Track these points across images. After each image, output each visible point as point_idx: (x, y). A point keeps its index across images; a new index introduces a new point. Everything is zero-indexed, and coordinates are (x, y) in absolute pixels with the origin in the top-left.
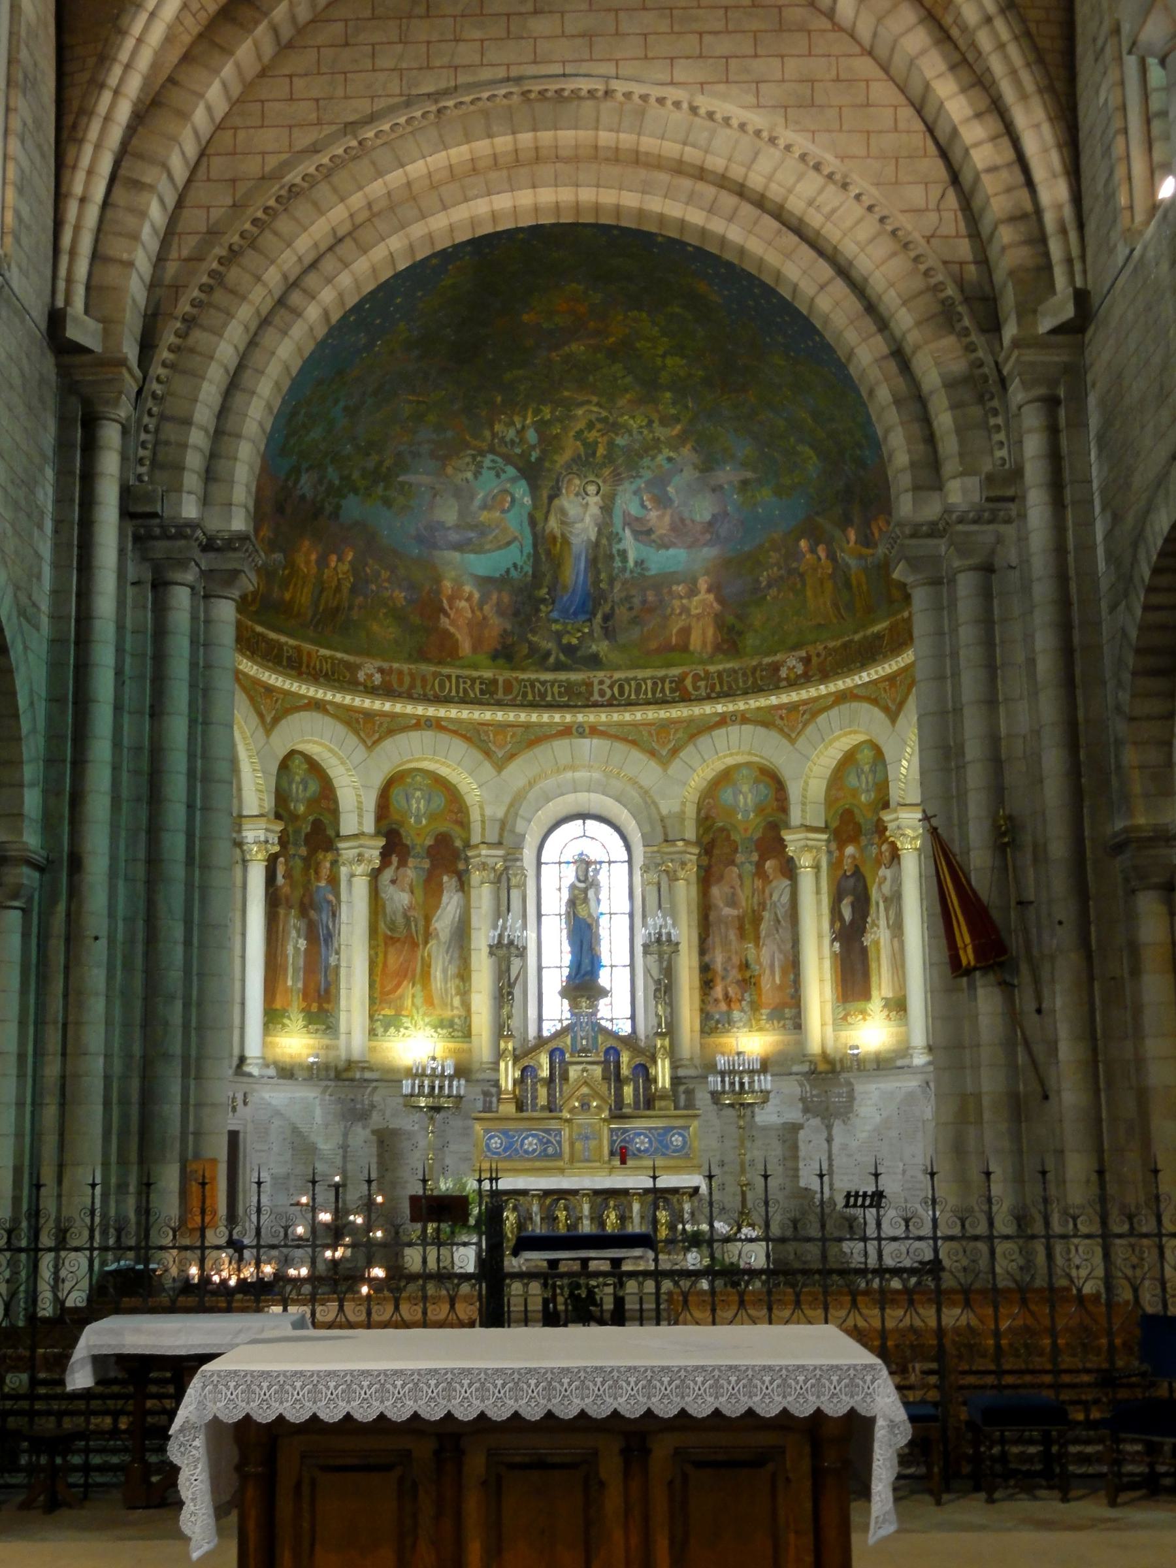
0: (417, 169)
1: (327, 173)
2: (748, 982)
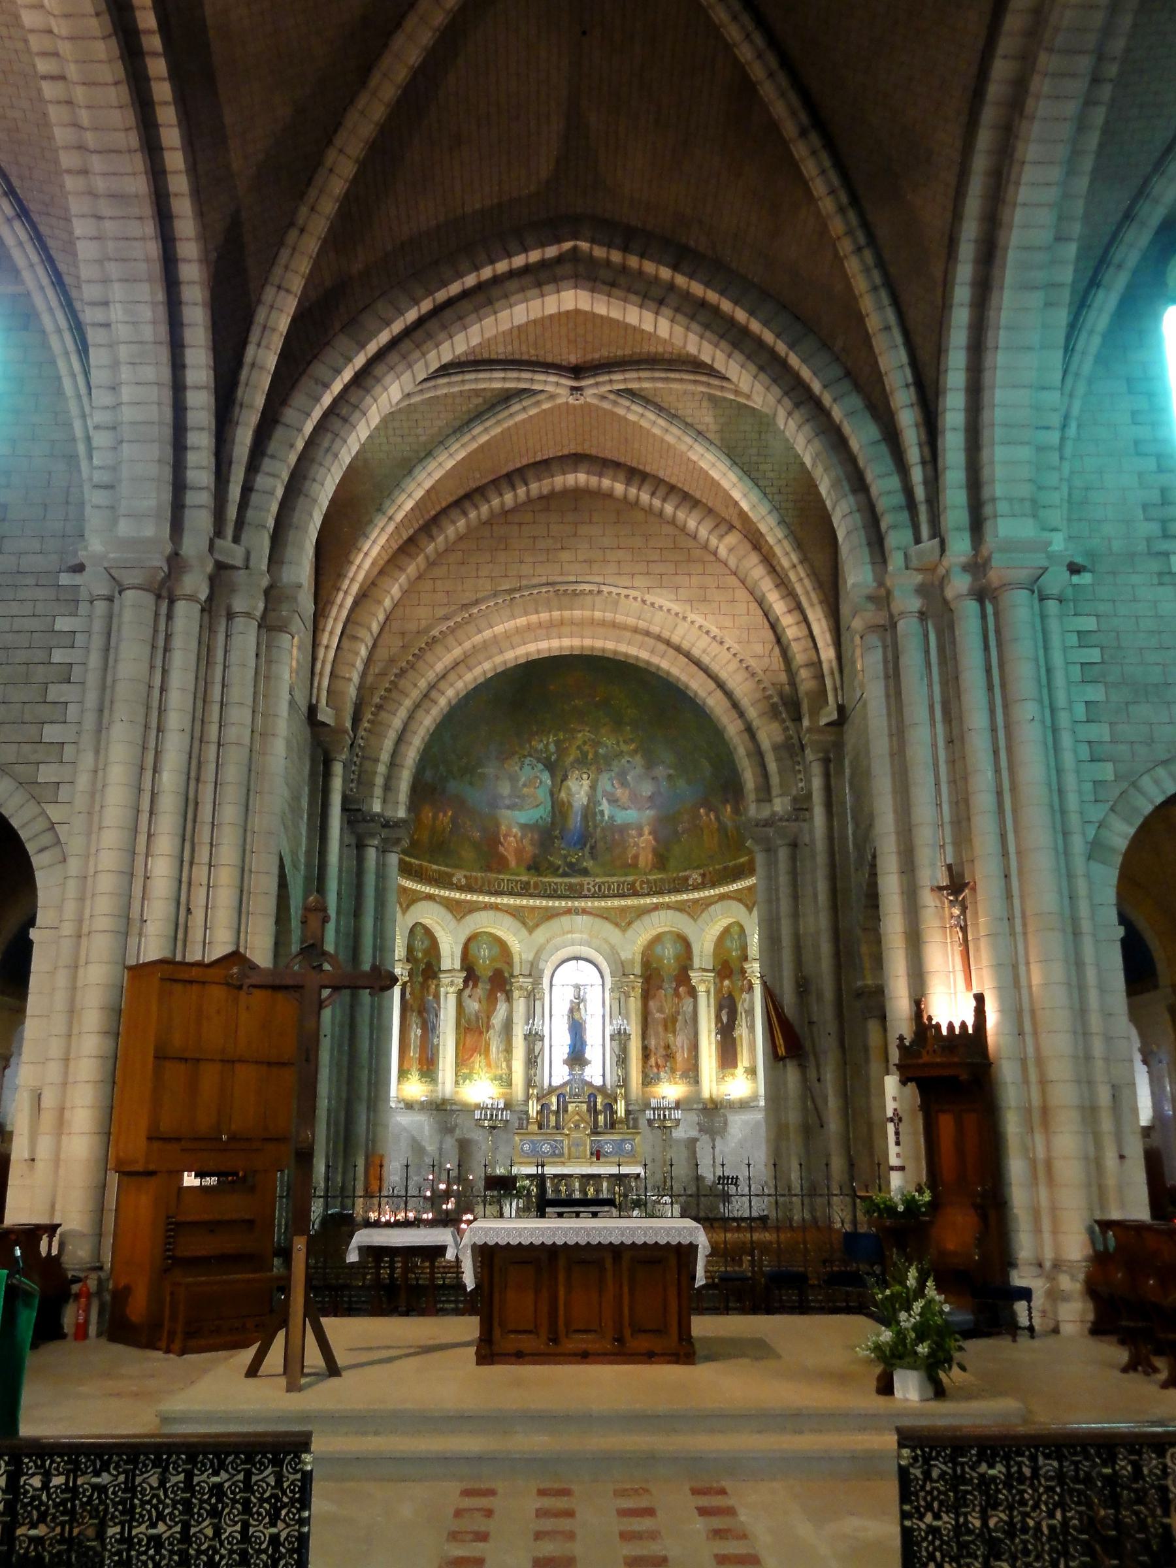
0: (499, 629)
1: (452, 630)
2: (669, 1056)
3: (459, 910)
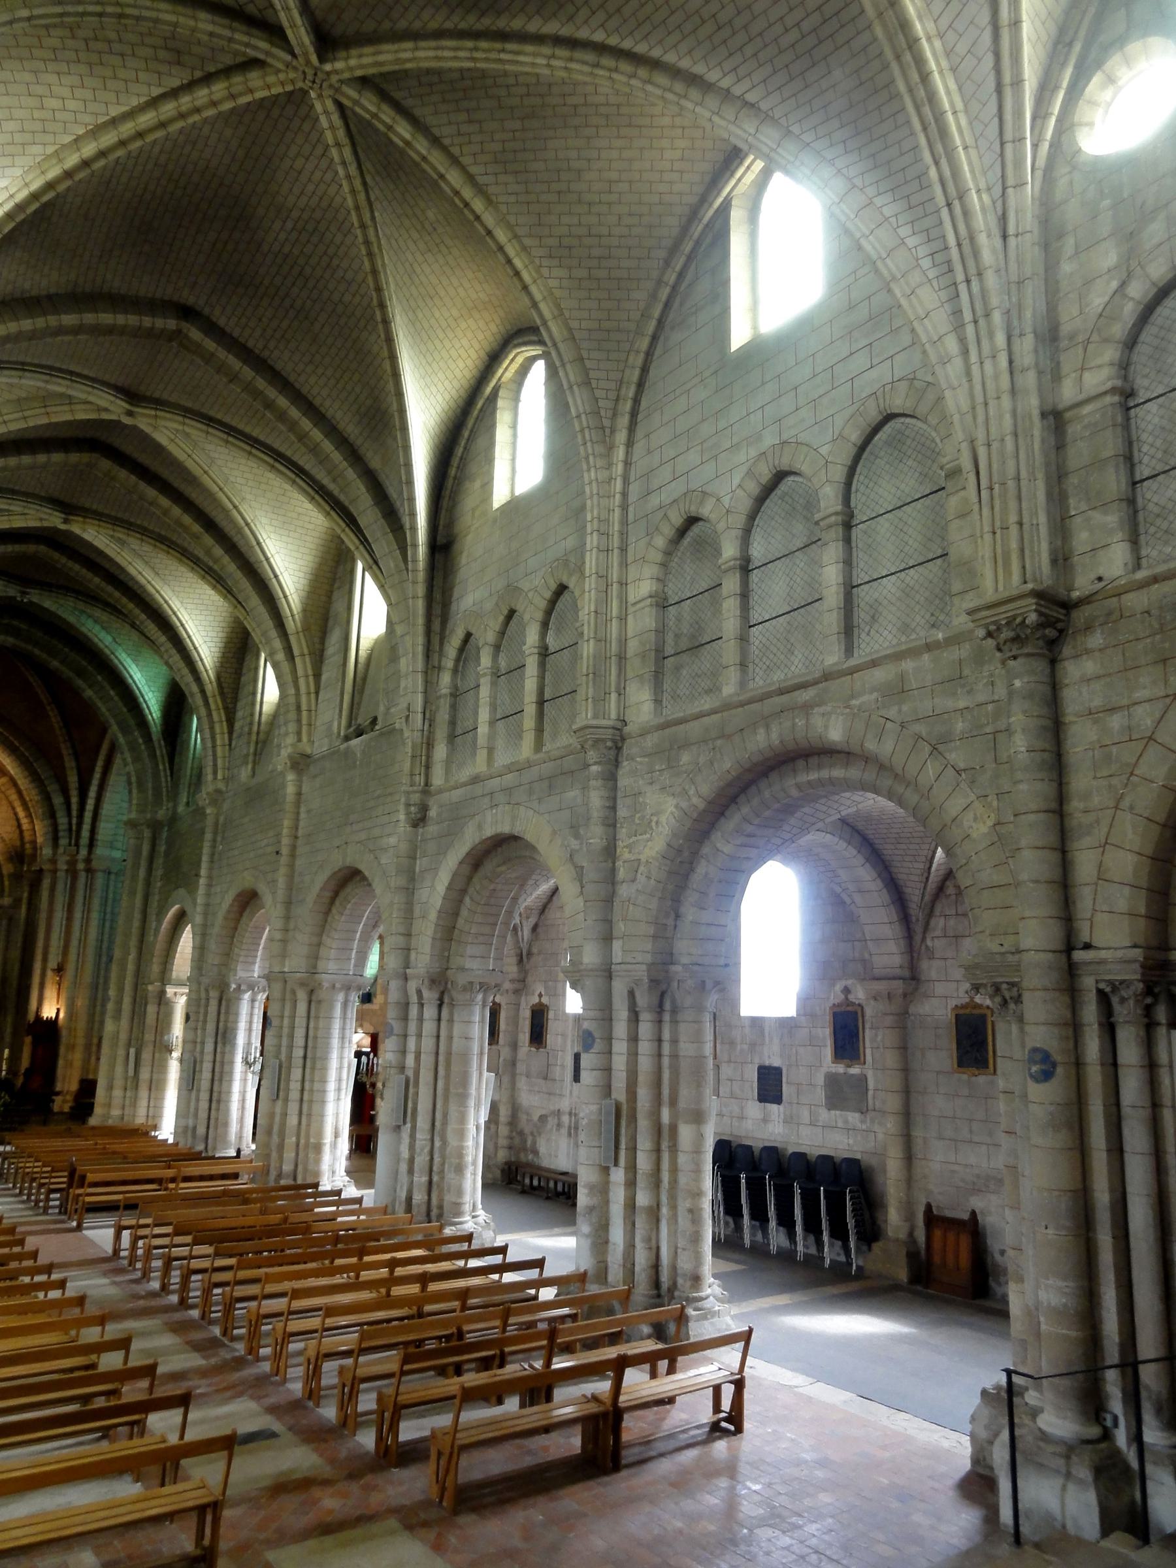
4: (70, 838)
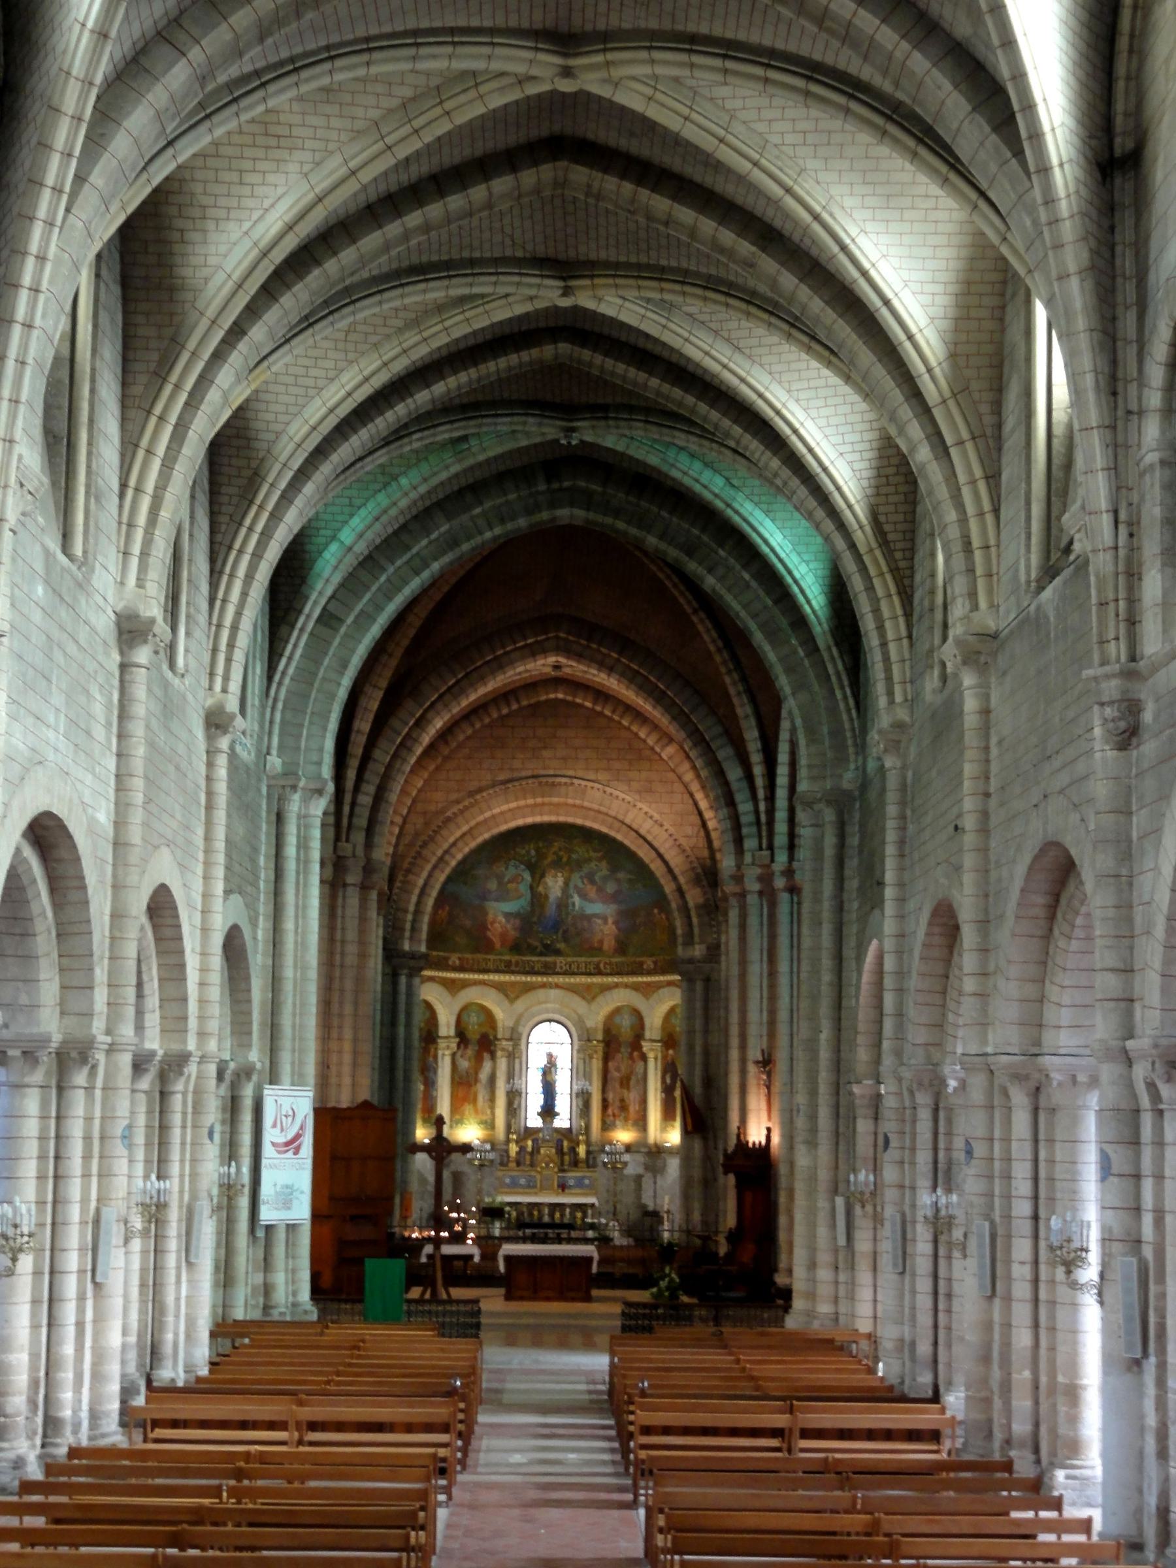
0: (496, 811)
1: (462, 812)
2: (624, 1107)
3: (453, 987)
4: (760, 837)
